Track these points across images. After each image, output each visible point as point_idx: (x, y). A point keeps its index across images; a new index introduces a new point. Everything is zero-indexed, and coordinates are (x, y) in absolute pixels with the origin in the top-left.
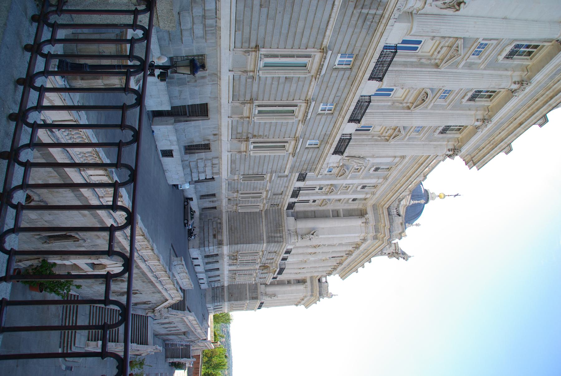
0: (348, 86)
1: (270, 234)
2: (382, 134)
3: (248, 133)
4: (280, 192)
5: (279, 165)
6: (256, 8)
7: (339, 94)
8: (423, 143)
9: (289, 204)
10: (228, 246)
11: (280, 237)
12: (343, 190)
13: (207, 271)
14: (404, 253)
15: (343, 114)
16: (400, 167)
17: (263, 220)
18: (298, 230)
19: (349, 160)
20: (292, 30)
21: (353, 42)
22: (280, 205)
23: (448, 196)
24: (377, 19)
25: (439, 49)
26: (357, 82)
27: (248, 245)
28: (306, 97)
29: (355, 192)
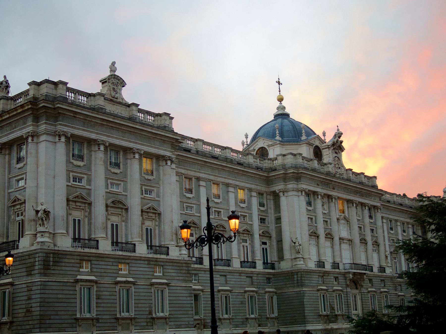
0: (104, 259)
1: (295, 285)
2: (154, 219)
4: (248, 279)
6: (51, 321)
8: (161, 185)
9: (265, 268)
10: (306, 325)
11: (297, 275)
12: (246, 220)
14: (335, 135)
15: (127, 257)
16: (212, 178)
17: (284, 292)
18: (293, 257)
20: (64, 300)
21: (71, 265)
22: (267, 276)
23: (280, 91)
25: (78, 207)
27: (305, 306)
28: (114, 284)
29: (249, 207)
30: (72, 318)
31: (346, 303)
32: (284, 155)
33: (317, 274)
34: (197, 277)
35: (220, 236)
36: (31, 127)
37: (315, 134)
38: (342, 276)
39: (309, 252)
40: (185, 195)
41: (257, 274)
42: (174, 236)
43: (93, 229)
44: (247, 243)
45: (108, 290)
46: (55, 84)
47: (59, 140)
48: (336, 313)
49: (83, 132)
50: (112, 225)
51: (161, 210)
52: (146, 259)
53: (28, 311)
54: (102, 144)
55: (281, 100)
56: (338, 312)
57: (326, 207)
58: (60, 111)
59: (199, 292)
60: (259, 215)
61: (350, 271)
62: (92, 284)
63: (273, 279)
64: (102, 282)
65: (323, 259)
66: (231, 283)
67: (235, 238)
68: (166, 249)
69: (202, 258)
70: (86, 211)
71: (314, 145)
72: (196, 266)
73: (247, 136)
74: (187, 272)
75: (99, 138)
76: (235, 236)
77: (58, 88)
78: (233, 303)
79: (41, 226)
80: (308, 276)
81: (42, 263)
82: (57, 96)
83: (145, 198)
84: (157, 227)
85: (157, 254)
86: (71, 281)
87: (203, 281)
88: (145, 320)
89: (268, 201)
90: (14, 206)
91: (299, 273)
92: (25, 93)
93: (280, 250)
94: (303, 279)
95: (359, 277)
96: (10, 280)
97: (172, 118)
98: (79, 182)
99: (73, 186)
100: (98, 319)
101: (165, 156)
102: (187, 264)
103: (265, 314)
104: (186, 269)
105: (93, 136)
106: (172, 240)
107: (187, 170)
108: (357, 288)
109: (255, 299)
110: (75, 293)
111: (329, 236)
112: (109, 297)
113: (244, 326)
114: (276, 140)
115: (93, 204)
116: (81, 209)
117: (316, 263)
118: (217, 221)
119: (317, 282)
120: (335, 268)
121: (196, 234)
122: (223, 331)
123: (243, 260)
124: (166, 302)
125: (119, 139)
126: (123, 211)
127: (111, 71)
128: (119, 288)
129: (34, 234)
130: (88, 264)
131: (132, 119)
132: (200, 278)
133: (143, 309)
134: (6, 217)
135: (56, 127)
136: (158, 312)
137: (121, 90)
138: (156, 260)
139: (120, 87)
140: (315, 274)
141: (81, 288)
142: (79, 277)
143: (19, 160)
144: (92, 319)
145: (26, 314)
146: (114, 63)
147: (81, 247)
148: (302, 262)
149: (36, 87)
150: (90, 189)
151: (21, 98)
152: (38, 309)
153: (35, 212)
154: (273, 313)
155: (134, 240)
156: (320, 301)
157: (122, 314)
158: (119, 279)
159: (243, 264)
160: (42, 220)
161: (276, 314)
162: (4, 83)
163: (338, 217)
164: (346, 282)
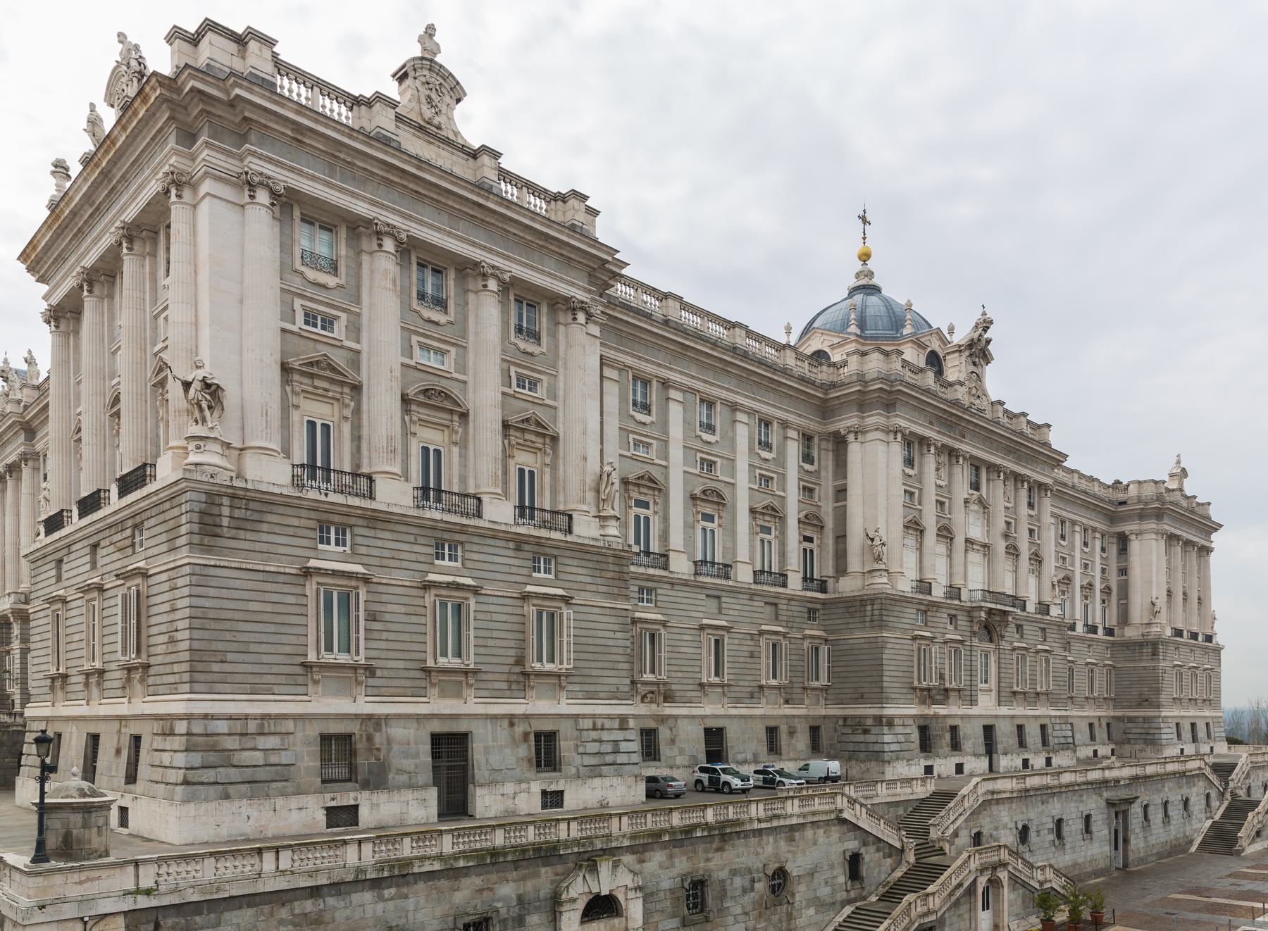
0: (391, 526)
1: (868, 624)
4: (769, 609)
9: (804, 589)
11: (873, 605)
13: (1195, 739)
18: (867, 569)
19: (604, 500)
21: (291, 531)
22: (810, 605)
26: (377, 515)
27: (885, 668)
31: (969, 668)
33: (915, 606)
38: (964, 613)
39: (901, 560)
41: (789, 600)
42: (590, 496)
48: (947, 685)
56: (951, 683)
59: (655, 627)
60: (800, 479)
63: (821, 612)
66: (731, 612)
69: (667, 556)
70: (347, 406)
72: (651, 571)
74: (617, 576)
78: (733, 653)
80: (896, 608)
81: (196, 517)
84: (547, 470)
93: (841, 556)
94: (884, 613)
102: (620, 558)
106: (583, 500)
108: (991, 641)
110: (302, 600)
113: (755, 701)
117: (914, 584)
118: (705, 480)
119: (913, 622)
120: (951, 598)
121: (655, 503)
123: (758, 567)
128: (432, 599)
130: (344, 534)
132: (660, 598)
138: (538, 542)
140: (910, 605)
152: (186, 634)
154: (817, 679)
159: (760, 578)
161: (824, 681)
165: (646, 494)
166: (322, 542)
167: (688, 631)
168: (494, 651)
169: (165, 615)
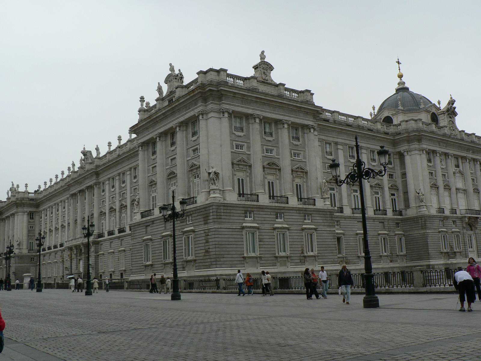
0: (264, 210)
2: (302, 177)
3: (300, 256)
4: (381, 224)
5: (327, 235)
6: (224, 259)
7: (269, 213)
8: (307, 149)
10: (430, 260)
14: (449, 103)
15: (282, 208)
18: (418, 205)
19: (324, 192)
20: (233, 243)
21: (238, 215)
22: (396, 221)
23: (399, 69)
24: (225, 208)
25: (241, 169)
27: (429, 245)
30: (241, 257)
32: (407, 121)
34: (339, 223)
35: (371, 172)
36: (201, 107)
37: (432, 103)
38: (459, 220)
40: (326, 157)
42: (319, 190)
43: (254, 186)
44: (378, 194)
45: (268, 234)
46: (218, 72)
47: (223, 115)
48: (455, 250)
49: (242, 108)
50: (269, 182)
51: (308, 169)
52: (297, 209)
53: (207, 252)
54: (257, 117)
55: (400, 76)
56: (456, 249)
57: (443, 163)
58: (222, 93)
59: (340, 235)
61: (466, 215)
62: (255, 230)
63: (401, 224)
64: (263, 228)
65: (443, 206)
67: (385, 172)
68: (313, 201)
71: (431, 112)
72: (338, 214)
73: (374, 108)
75: (255, 113)
76: (385, 170)
77: (220, 75)
79: (213, 185)
80: (431, 220)
82: (220, 81)
83: (294, 160)
84: (305, 184)
85: (306, 205)
86: (238, 227)
87: (344, 227)
88: (299, 258)
89: (395, 160)
90: (192, 170)
91: (423, 218)
92: (195, 81)
95: (473, 220)
96: (192, 228)
97: (313, 94)
98: (240, 149)
99: (236, 152)
100: (260, 257)
101: (309, 125)
102: (331, 212)
103: (395, 252)
104: (330, 216)
105: (250, 111)
106: (318, 194)
107: (327, 136)
108: (472, 230)
109: (387, 240)
111: (447, 187)
112: (269, 240)
113: (379, 262)
114: (399, 110)
115: (252, 166)
116: (244, 170)
117: (437, 210)
119: (438, 225)
121: (336, 188)
122: (361, 266)
124: (315, 244)
125: (270, 113)
126: (277, 171)
127: (261, 58)
129: (208, 192)
130: (251, 214)
131: (280, 96)
132: (341, 224)
133: (297, 249)
134: (186, 179)
135: (221, 106)
136: (309, 251)
137: (270, 73)
138: (306, 209)
139: (269, 71)
141: (246, 233)
142: (244, 225)
143: (194, 134)
144: (257, 258)
145: (205, 254)
146: (263, 52)
147: (245, 200)
148: (425, 209)
149: (203, 75)
150: (250, 155)
151: (192, 85)
153: (207, 174)
154: (402, 252)
155: (286, 194)
156: (441, 241)
157: (280, 253)
158: (276, 226)
160: (214, 180)
161: (404, 252)
162: (179, 75)
163: (454, 171)
164: (462, 225)
165: (333, 185)
166: (246, 217)
167: (352, 236)
168: (295, 249)
169: (204, 244)
